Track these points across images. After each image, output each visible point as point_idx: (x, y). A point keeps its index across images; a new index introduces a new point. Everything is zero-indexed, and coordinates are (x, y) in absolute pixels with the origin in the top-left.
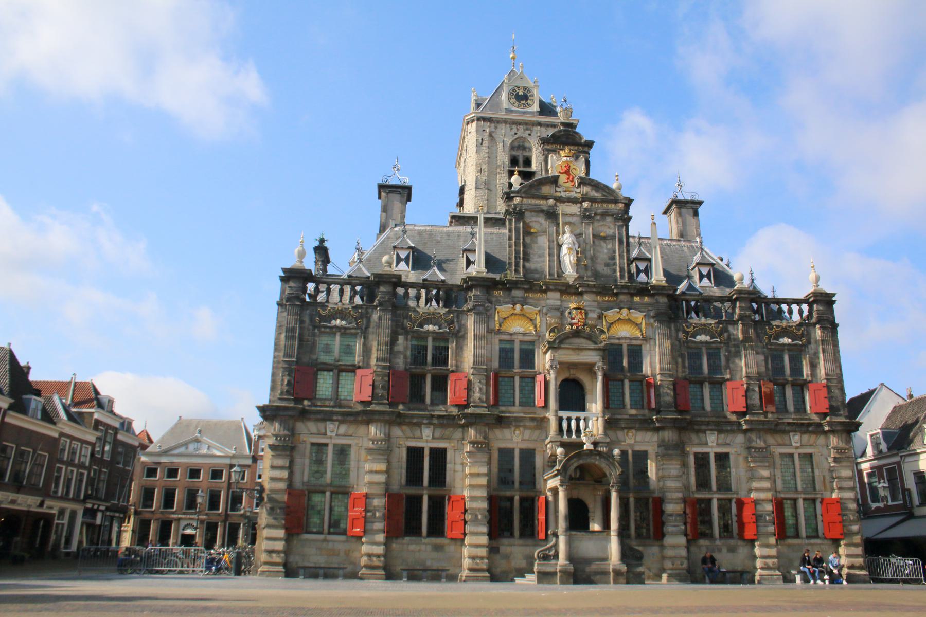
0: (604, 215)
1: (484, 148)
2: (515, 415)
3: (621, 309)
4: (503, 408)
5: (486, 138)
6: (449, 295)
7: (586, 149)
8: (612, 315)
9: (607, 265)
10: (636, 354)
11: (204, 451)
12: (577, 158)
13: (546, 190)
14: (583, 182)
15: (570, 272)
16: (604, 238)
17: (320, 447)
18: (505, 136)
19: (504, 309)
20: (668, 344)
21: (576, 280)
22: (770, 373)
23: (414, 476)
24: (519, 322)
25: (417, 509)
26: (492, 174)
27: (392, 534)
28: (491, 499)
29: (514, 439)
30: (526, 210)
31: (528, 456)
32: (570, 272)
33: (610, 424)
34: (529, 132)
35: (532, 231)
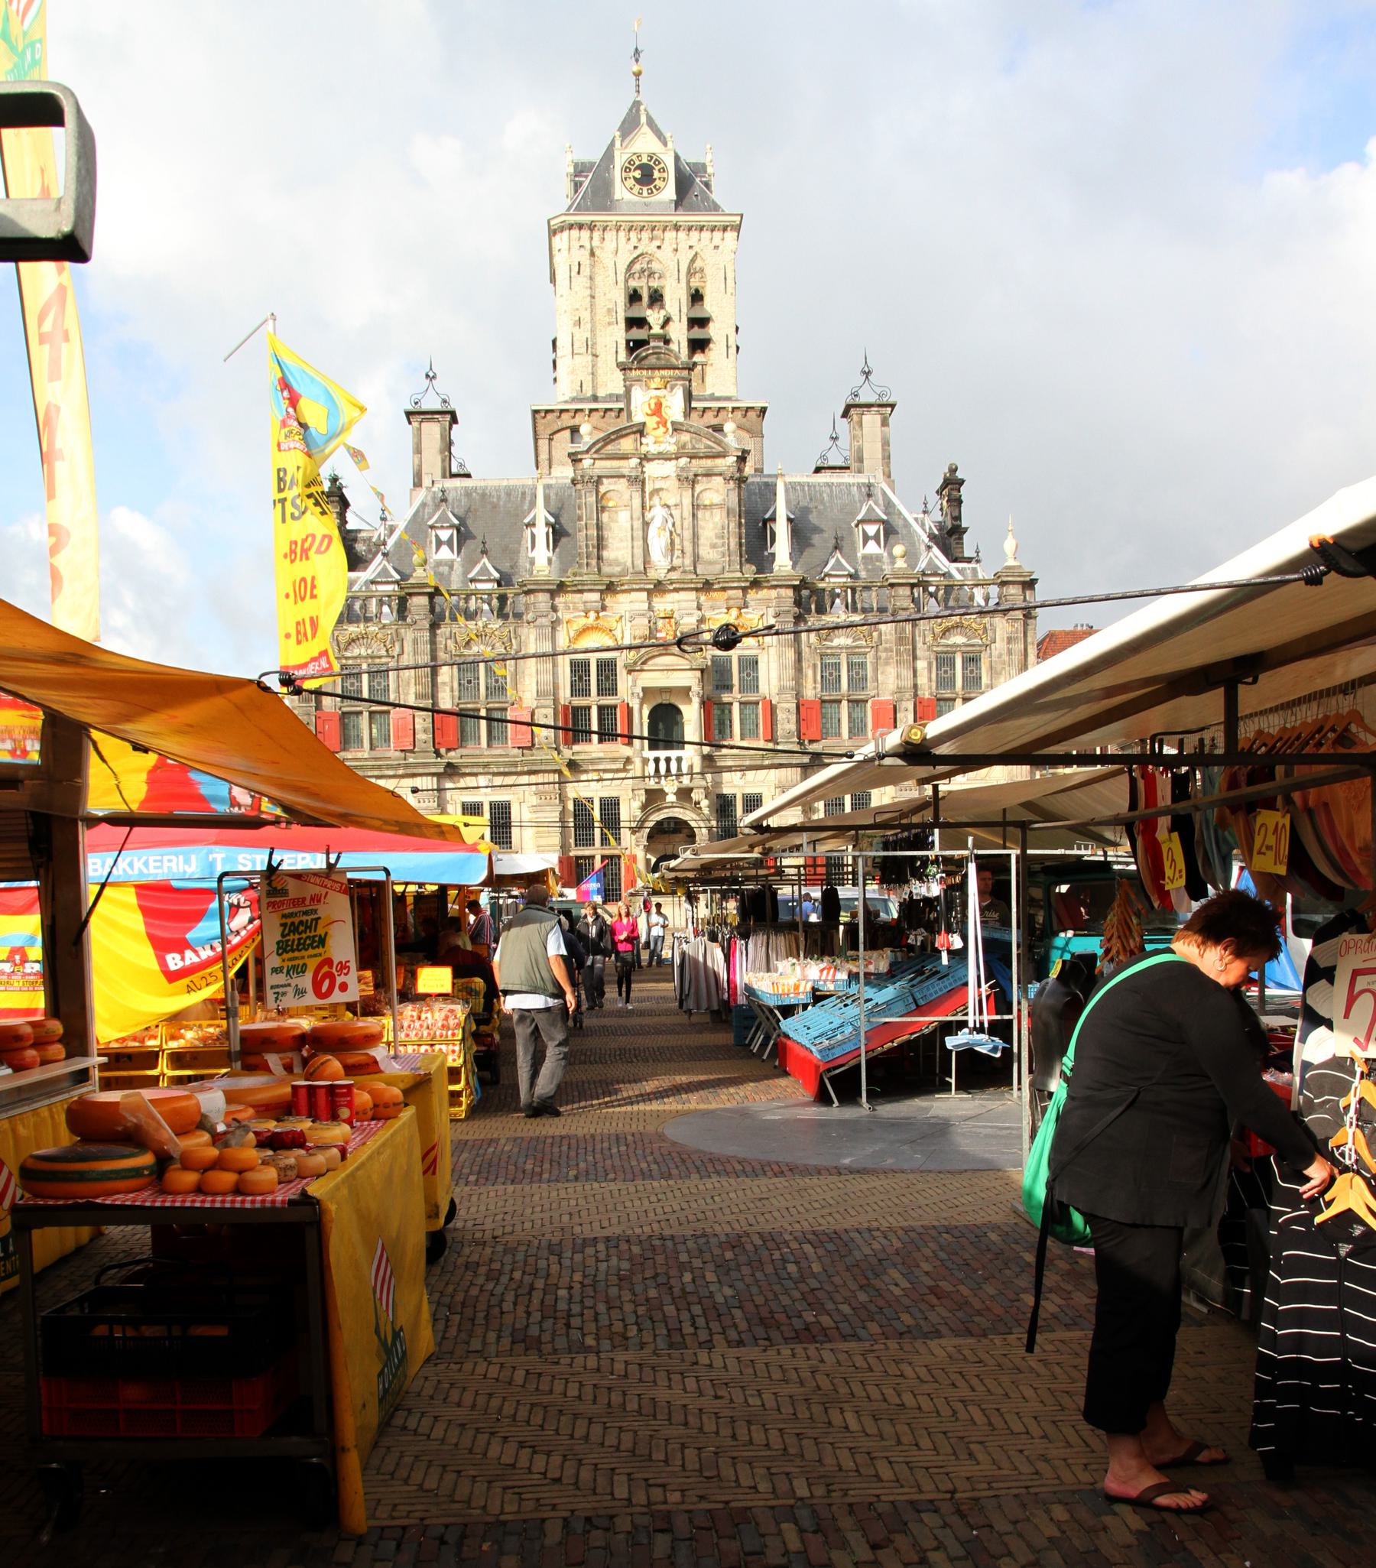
0: (708, 475)
1: (582, 282)
2: (594, 755)
3: (728, 609)
4: (576, 748)
5: (586, 260)
7: (685, 373)
9: (714, 546)
12: (672, 389)
13: (627, 444)
14: (677, 428)
16: (712, 506)
21: (669, 571)
22: (934, 684)
30: (600, 477)
31: (610, 807)
34: (657, 243)
35: (611, 504)
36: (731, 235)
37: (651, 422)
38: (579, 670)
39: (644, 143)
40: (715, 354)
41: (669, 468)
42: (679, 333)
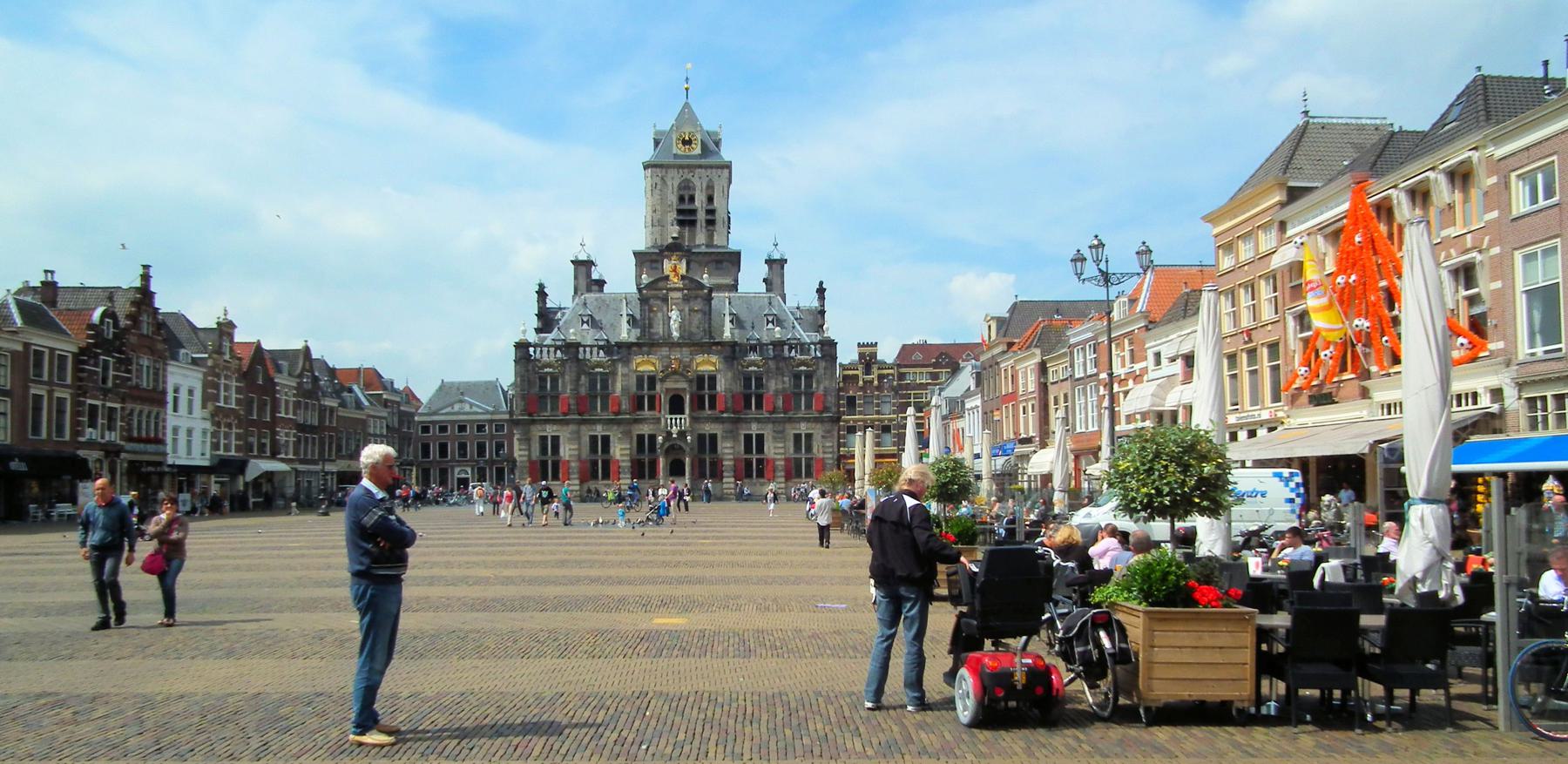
6: (608, 348)
8: (699, 358)
10: (713, 379)
11: (467, 408)
13: (661, 284)
14: (683, 278)
15: (676, 334)
17: (543, 439)
18: (674, 179)
19: (639, 359)
20: (730, 375)
23: (593, 449)
24: (646, 365)
25: (597, 468)
26: (664, 213)
27: (582, 481)
28: (632, 461)
29: (646, 429)
31: (653, 438)
32: (676, 334)
33: (694, 419)
36: (726, 171)
37: (672, 275)
38: (640, 379)
39: (686, 132)
40: (719, 226)
41: (678, 295)
42: (701, 216)
